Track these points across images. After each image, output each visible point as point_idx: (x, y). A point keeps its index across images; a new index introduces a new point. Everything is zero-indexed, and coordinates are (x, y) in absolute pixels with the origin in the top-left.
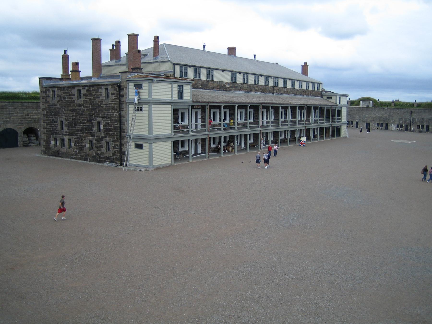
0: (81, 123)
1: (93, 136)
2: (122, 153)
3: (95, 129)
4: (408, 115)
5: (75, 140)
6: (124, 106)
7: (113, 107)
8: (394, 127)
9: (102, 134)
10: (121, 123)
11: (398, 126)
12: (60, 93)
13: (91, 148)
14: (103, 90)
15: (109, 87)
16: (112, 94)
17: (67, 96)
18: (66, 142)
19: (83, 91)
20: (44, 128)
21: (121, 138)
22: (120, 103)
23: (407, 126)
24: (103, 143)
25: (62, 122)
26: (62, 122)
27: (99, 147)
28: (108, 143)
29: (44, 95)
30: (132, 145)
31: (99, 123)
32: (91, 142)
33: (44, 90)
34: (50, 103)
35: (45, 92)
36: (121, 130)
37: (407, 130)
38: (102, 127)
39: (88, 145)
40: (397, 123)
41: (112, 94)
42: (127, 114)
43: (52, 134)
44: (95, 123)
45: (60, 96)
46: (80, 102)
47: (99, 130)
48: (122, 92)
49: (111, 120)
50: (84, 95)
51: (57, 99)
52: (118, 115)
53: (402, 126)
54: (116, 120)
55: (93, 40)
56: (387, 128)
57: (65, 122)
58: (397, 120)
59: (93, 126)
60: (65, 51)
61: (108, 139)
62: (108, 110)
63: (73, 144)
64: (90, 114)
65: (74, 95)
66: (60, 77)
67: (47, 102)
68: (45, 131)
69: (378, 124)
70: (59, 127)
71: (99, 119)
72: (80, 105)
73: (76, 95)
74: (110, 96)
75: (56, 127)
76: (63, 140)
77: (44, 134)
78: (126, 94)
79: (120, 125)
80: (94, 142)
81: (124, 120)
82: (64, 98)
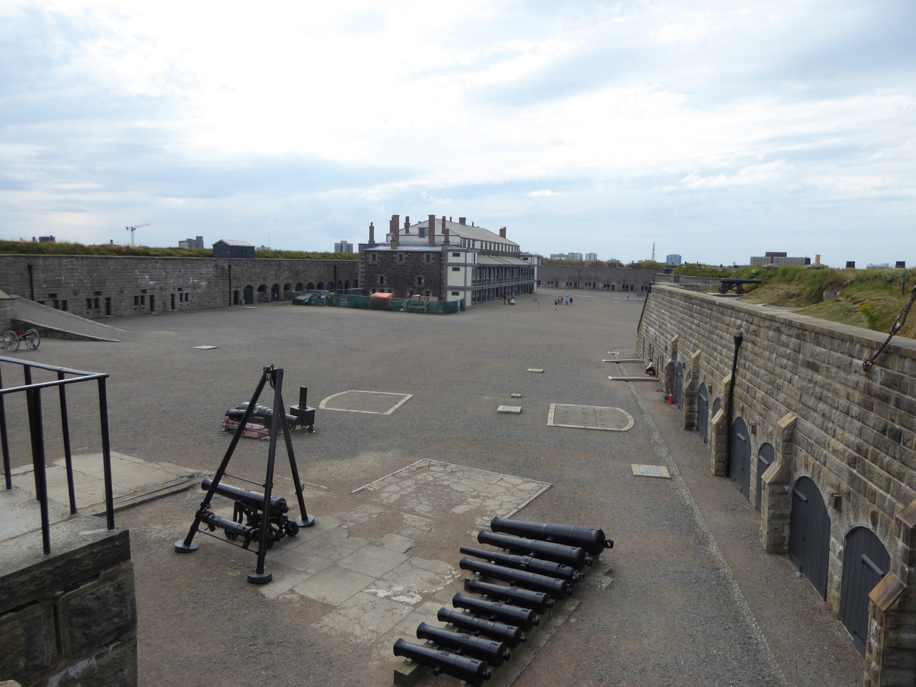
1: (414, 287)
3: (416, 283)
8: (563, 285)
10: (441, 279)
14: (425, 256)
15: (431, 255)
21: (441, 288)
22: (441, 265)
25: (382, 278)
26: (382, 278)
30: (449, 293)
31: (420, 279)
38: (423, 281)
42: (446, 273)
44: (416, 278)
46: (401, 263)
47: (420, 283)
51: (377, 261)
56: (557, 286)
57: (385, 278)
67: (366, 262)
69: (549, 283)
70: (379, 281)
78: (447, 259)
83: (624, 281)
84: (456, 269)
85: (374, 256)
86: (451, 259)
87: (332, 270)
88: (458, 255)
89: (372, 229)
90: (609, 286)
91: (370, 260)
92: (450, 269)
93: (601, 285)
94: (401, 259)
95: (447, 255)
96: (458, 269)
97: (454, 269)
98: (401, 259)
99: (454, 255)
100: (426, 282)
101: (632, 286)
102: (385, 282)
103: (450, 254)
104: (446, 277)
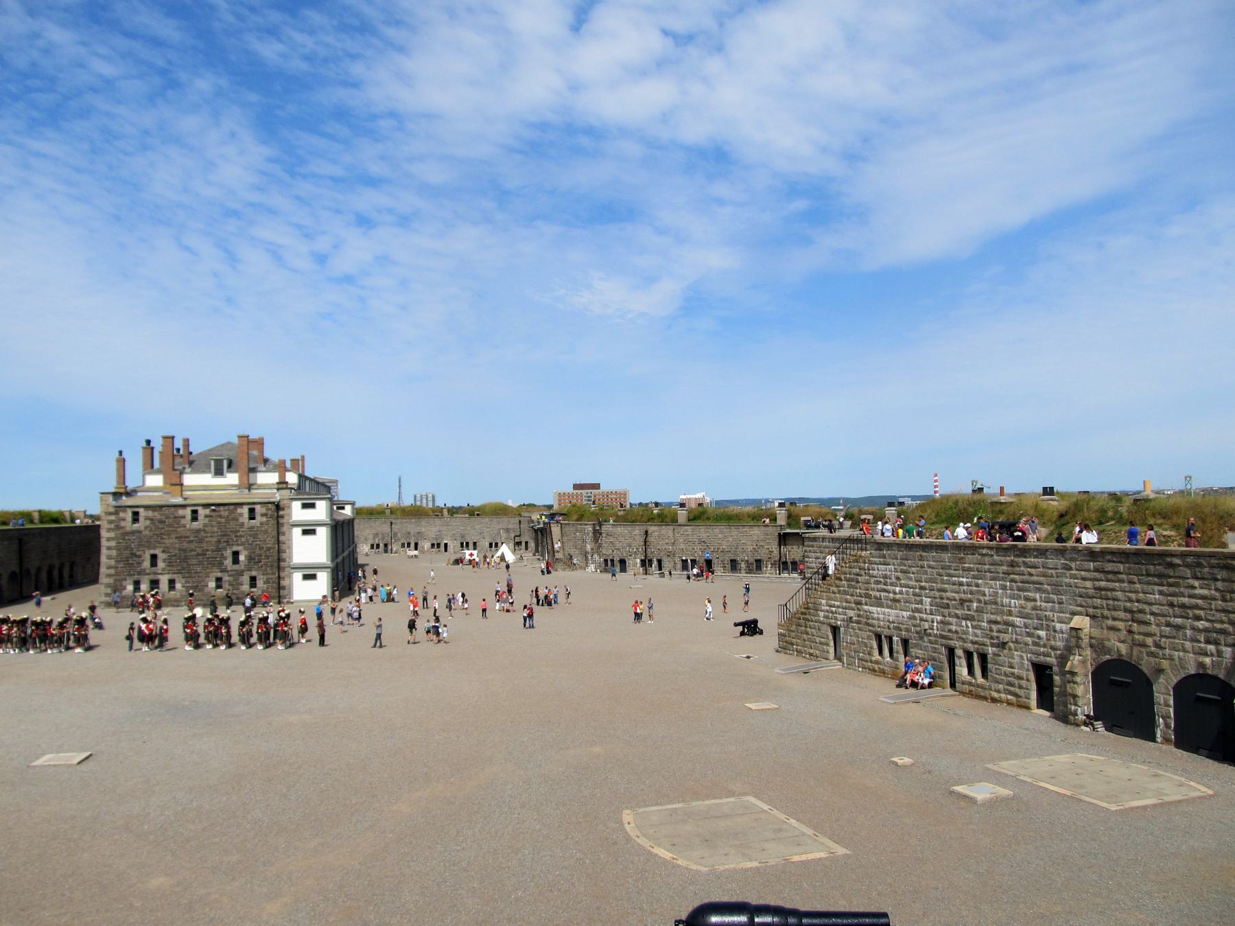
0: (198, 555)
2: (280, 588)
3: (228, 562)
4: (386, 528)
5: (183, 581)
6: (284, 529)
7: (266, 532)
9: (241, 566)
11: (372, 546)
12: (150, 513)
13: (219, 587)
14: (245, 510)
15: (258, 508)
16: (262, 515)
17: (168, 518)
18: (164, 585)
19: (202, 512)
20: (109, 568)
22: (279, 526)
23: (386, 545)
24: (246, 579)
25: (154, 557)
26: (154, 557)
27: (236, 584)
28: (253, 579)
29: (113, 518)
30: (297, 577)
32: (219, 580)
33: (112, 510)
34: (128, 529)
35: (116, 513)
36: (279, 560)
37: (386, 551)
38: (242, 558)
39: (212, 584)
40: (371, 542)
41: (262, 515)
42: (290, 540)
43: (130, 575)
44: (228, 553)
45: (151, 520)
47: (236, 560)
48: (281, 513)
49: (261, 548)
50: (206, 516)
52: (273, 540)
53: (378, 546)
54: (269, 549)
55: (165, 438)
58: (371, 537)
59: (225, 558)
60: (121, 453)
61: (254, 573)
62: (255, 536)
63: (178, 586)
64: (219, 542)
65: (184, 517)
66: (113, 490)
67: (118, 527)
68: (112, 571)
71: (235, 548)
72: (198, 531)
73: (189, 517)
74: (258, 517)
75: (140, 564)
76: (155, 584)
77: (109, 576)
78: (290, 515)
79: (279, 552)
80: (226, 578)
81: (283, 547)
82: (161, 522)
83: (463, 536)
84: (309, 531)
85: (136, 514)
86: (297, 512)
87: (15, 547)
88: (312, 506)
89: (122, 462)
90: (439, 545)
91: (128, 524)
92: (297, 532)
93: (427, 545)
94: (195, 519)
95: (289, 507)
96: (313, 532)
97: (305, 532)
98: (195, 519)
99: (305, 506)
100: (250, 558)
101: (475, 544)
102: (161, 564)
103: (296, 505)
104: (290, 547)
